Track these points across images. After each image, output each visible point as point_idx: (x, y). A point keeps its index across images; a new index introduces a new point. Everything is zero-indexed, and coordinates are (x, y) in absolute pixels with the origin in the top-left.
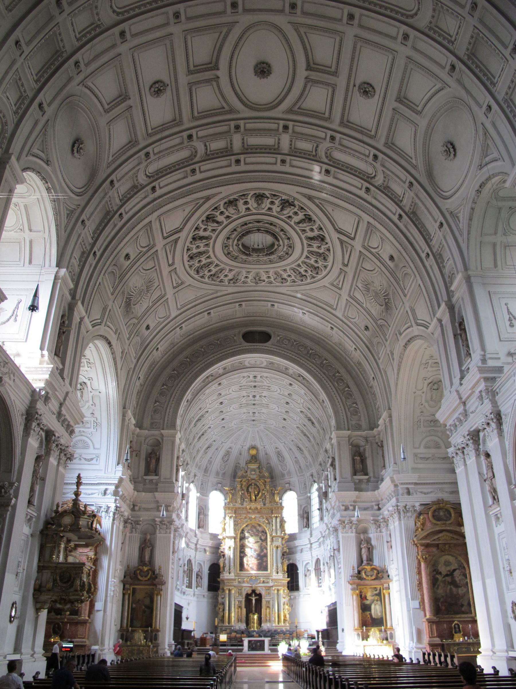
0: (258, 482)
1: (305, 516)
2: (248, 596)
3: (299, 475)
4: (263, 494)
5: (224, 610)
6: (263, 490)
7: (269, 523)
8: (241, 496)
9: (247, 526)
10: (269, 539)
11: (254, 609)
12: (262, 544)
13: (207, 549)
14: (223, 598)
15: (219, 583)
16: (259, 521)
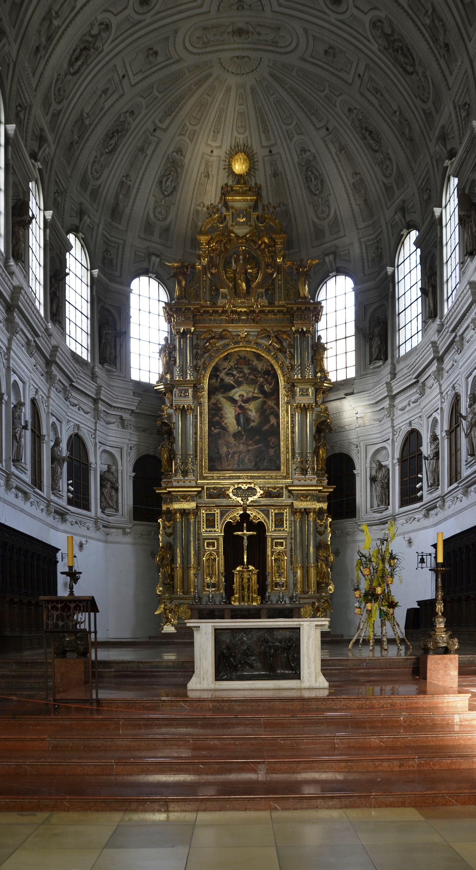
0: (255, 243)
1: (376, 330)
2: (229, 528)
3: (362, 225)
4: (267, 276)
5: (173, 560)
6: (267, 265)
7: (282, 350)
8: (211, 280)
9: (226, 358)
10: (282, 392)
11: (245, 560)
12: (264, 403)
13: (126, 416)
14: (169, 535)
15: (159, 499)
16: (257, 344)
